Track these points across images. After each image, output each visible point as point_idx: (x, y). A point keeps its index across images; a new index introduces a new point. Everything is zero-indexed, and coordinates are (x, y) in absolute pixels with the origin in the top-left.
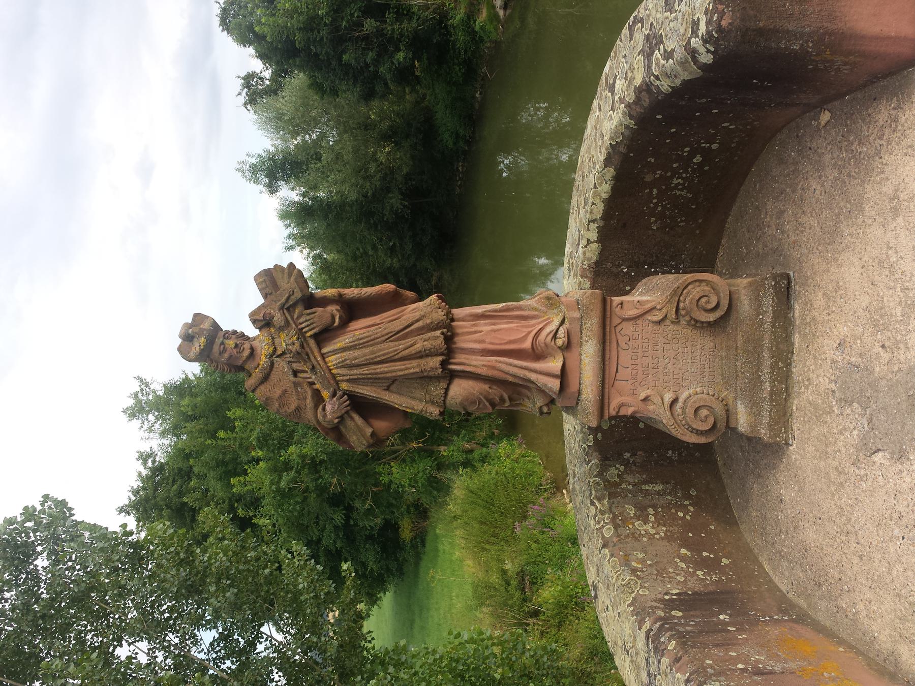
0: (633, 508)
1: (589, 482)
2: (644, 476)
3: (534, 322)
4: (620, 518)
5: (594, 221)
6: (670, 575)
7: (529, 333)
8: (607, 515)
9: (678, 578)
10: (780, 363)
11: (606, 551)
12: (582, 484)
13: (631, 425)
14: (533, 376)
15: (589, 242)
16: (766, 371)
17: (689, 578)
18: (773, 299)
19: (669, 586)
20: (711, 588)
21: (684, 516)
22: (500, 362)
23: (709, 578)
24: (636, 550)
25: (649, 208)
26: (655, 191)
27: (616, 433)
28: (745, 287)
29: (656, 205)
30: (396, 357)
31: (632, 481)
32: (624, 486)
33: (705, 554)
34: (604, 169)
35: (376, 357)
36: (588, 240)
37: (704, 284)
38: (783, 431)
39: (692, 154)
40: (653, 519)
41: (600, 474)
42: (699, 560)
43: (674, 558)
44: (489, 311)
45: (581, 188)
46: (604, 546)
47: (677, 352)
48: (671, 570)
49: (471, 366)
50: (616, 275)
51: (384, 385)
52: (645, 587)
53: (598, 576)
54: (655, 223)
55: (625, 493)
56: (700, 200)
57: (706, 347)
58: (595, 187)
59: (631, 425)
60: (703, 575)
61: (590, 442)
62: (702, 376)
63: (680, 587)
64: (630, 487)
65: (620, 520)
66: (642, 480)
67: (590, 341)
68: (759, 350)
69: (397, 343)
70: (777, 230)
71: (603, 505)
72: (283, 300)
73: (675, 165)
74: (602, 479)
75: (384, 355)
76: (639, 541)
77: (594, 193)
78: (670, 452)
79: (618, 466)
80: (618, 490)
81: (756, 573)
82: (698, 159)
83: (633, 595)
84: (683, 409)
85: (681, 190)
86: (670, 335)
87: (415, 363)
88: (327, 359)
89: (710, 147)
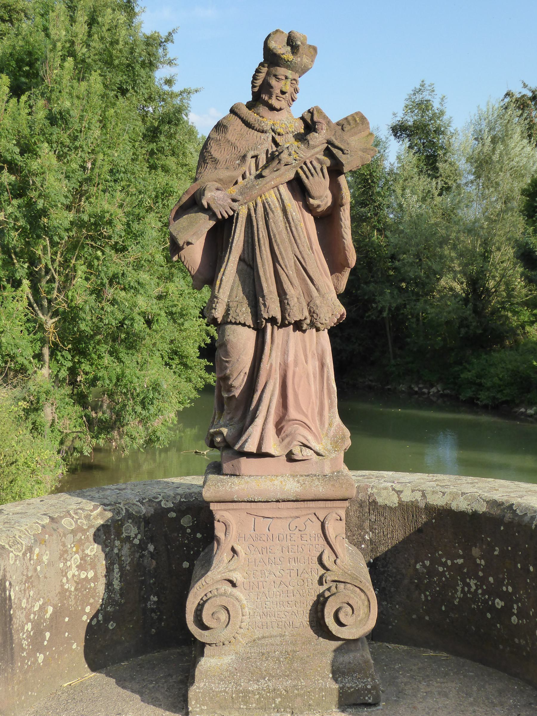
0: (93, 553)
1: (120, 503)
2: (128, 568)
3: (318, 423)
4: (83, 537)
5: (424, 496)
6: (27, 592)
7: (306, 416)
8: (85, 522)
9: (25, 601)
10: (280, 699)
11: (47, 520)
12: (113, 496)
13: (186, 552)
14: (259, 421)
15: (399, 492)
16: (270, 684)
17: (24, 613)
18: (352, 687)
19: (17, 588)
20: (15, 637)
21: (86, 613)
22: (275, 384)
23: (24, 636)
24: (50, 554)
25: (441, 556)
26: (460, 561)
27: (176, 535)
28: (363, 656)
29: (444, 565)
30: (279, 267)
31: (123, 553)
32: (117, 543)
33: (48, 635)
34: (484, 501)
35: (278, 245)
36: (402, 492)
37: (366, 610)
38: (203, 707)
39: (503, 596)
40: (83, 576)
41: (129, 515)
42: (42, 627)
43: (43, 598)
44: (328, 372)
45: (459, 482)
46: (52, 519)
47: (287, 584)
48: (32, 593)
49: (271, 350)
50: (361, 527)
51: (246, 255)
52: (16, 560)
53: (13, 514)
54: (424, 566)
55: (109, 545)
56: (452, 615)
57: (294, 616)
58: (463, 494)
59: (186, 552)
60: (27, 630)
61: (165, 504)
62: (261, 614)
63: (16, 602)
64: (116, 551)
65: (81, 537)
66: (125, 565)
67: (299, 485)
68: (294, 675)
69: (293, 268)
70: (426, 693)
71: (95, 518)
72: (337, 143)
73: (491, 579)
74: (124, 517)
75: (281, 253)
76: (60, 558)
77: (457, 494)
78: (156, 599)
79: (139, 536)
80: (113, 537)
81: (30, 693)
82: (499, 603)
83: (7, 546)
84: (225, 594)
85: (463, 591)
86: (307, 576)
87: (273, 288)
88: (272, 191)
89: (514, 614)
